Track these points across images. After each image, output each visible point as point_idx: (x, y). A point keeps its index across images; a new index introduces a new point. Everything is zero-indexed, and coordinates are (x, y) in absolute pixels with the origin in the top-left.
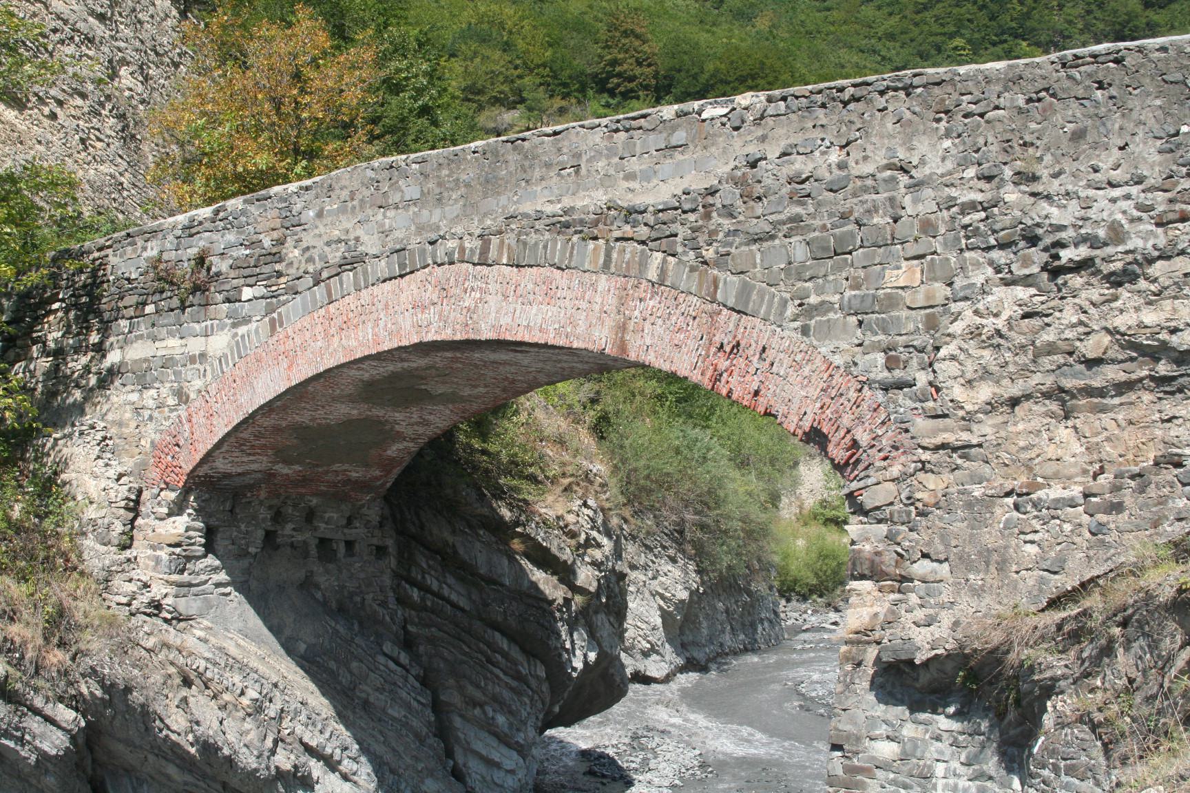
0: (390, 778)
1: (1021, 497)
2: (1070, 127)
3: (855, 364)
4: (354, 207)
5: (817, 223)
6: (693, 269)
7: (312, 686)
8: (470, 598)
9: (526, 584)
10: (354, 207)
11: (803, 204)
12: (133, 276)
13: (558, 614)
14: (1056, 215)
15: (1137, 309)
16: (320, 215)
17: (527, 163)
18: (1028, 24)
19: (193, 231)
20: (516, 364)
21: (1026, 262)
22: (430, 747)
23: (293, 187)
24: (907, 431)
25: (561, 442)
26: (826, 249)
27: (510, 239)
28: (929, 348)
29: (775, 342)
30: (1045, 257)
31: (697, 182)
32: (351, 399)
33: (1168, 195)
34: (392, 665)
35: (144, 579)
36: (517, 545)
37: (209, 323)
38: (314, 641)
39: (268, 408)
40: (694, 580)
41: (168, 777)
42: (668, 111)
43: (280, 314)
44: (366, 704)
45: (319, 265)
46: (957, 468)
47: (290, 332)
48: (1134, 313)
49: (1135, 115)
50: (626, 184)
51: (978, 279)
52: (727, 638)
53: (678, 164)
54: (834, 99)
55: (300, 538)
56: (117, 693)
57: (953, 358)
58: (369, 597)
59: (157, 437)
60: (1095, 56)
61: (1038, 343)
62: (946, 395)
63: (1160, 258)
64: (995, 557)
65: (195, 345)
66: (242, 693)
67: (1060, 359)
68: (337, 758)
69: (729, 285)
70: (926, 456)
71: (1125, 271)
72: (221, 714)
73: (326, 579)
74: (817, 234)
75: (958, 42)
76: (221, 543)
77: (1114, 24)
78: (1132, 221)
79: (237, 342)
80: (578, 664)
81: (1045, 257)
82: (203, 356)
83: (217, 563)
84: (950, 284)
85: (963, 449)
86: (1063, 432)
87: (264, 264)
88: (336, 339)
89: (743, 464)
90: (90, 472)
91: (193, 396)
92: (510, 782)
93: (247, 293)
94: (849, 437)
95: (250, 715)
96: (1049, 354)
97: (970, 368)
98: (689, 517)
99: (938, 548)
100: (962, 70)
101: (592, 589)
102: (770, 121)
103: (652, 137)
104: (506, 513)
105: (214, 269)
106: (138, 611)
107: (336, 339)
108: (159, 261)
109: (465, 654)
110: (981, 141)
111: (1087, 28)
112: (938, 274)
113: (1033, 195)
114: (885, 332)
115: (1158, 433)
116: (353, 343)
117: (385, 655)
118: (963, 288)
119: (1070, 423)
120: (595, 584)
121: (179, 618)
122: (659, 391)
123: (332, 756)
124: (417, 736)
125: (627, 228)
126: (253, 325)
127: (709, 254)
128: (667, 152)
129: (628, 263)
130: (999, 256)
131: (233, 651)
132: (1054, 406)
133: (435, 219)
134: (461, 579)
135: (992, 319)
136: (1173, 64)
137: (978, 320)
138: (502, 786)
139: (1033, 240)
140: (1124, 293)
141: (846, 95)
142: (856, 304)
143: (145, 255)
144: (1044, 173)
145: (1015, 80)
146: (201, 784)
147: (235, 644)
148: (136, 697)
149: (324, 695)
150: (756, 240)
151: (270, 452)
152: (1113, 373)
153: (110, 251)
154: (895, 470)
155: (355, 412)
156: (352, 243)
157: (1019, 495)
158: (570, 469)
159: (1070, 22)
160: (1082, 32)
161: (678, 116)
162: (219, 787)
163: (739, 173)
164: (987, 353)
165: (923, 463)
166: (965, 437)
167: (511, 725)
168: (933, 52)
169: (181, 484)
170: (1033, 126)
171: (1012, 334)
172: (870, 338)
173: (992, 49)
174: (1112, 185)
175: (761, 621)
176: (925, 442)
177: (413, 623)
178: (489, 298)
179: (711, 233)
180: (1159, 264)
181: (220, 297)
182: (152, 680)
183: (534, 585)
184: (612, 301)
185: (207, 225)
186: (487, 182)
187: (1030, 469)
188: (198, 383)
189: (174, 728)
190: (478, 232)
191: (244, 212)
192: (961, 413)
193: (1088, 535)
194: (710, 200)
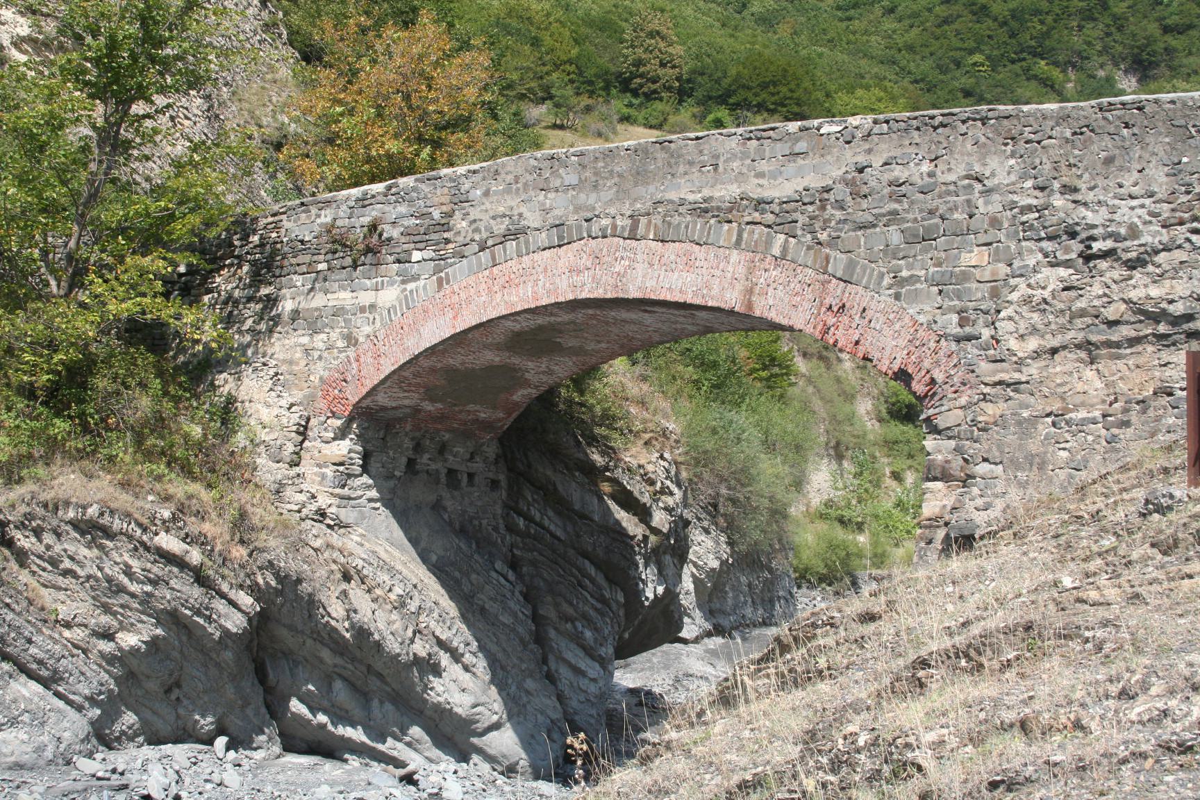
0: (501, 674)
1: (1057, 417)
2: (1103, 155)
3: (935, 322)
4: (518, 189)
5: (910, 216)
6: (809, 248)
7: (443, 591)
8: (565, 530)
9: (612, 521)
10: (518, 189)
11: (900, 202)
12: (307, 239)
13: (637, 549)
14: (1091, 217)
15: (1146, 286)
16: (487, 194)
17: (673, 161)
18: (1047, 43)
19: (366, 202)
20: (640, 323)
21: (1067, 250)
22: (531, 651)
23: (461, 170)
24: (973, 371)
25: (642, 403)
26: (916, 236)
27: (657, 220)
28: (993, 311)
29: (873, 305)
30: (1081, 247)
31: (815, 182)
32: (498, 347)
33: (1172, 206)
34: (502, 581)
35: (313, 491)
36: (606, 487)
37: (380, 279)
38: (443, 553)
39: (431, 351)
40: (725, 551)
41: (321, 661)
42: (793, 126)
43: (447, 274)
44: (483, 610)
45: (484, 235)
46: (1010, 399)
47: (456, 287)
48: (1143, 288)
49: (1150, 148)
50: (756, 181)
51: (1031, 262)
52: (748, 611)
53: (800, 168)
54: (926, 125)
55: (433, 466)
56: (289, 583)
57: (1010, 318)
58: (484, 522)
59: (326, 374)
60: (1123, 104)
61: (1073, 309)
62: (1004, 346)
63: (1163, 250)
64: (1037, 460)
65: (366, 298)
66: (390, 590)
67: (1089, 320)
68: (461, 651)
69: (838, 262)
70: (987, 390)
71: (1138, 259)
72: (374, 606)
74: (909, 224)
75: (978, 58)
76: (374, 465)
77: (1132, 47)
78: (1145, 223)
79: (406, 296)
80: (651, 596)
81: (1081, 247)
82: (373, 307)
83: (371, 482)
84: (1010, 265)
85: (1015, 385)
86: (1089, 374)
87: (433, 233)
89: (769, 446)
90: (264, 401)
91: (361, 339)
93: (416, 256)
94: (928, 376)
95: (396, 608)
96: (1081, 316)
97: (1023, 326)
98: (724, 491)
99: (995, 454)
100: (1025, 108)
101: (665, 530)
102: (875, 138)
103: (779, 145)
104: (597, 458)
105: (385, 235)
106: (307, 517)
107: (499, 295)
108: (333, 226)
109: (560, 576)
110: (1037, 161)
111: (1105, 50)
112: (1002, 257)
113: (1074, 202)
114: (959, 299)
115: (1157, 374)
117: (497, 571)
118: (1019, 268)
119: (1094, 367)
120: (667, 526)
121: (340, 525)
122: (695, 377)
123: (457, 649)
124: (522, 640)
125: (757, 214)
126: (421, 283)
127: (823, 236)
128: (791, 158)
129: (756, 242)
130: (1044, 244)
131: (383, 555)
132: (1083, 355)
133: (591, 201)
134: (559, 514)
135: (1040, 291)
136: (1179, 113)
137: (1030, 291)
138: (585, 692)
139: (1073, 235)
140: (1137, 274)
141: (936, 122)
142: (937, 278)
143: (319, 221)
144: (1083, 187)
145: (1064, 118)
146: (350, 666)
147: (384, 550)
148: (305, 588)
149: (451, 598)
150: (862, 227)
151: (422, 390)
152: (1126, 331)
153: (284, 217)
154: (963, 400)
155: (497, 359)
156: (516, 218)
157: (1056, 416)
158: (651, 426)
159: (1089, 44)
160: (1100, 53)
161: (801, 130)
162: (364, 669)
163: (850, 177)
164: (1035, 316)
165: (984, 395)
166: (1017, 376)
167: (596, 640)
168: (952, 66)
169: (347, 413)
170: (1076, 152)
171: (1055, 302)
172: (947, 303)
173: (1010, 67)
174: (1131, 197)
175: (779, 598)
176: (987, 380)
177: (518, 548)
178: (636, 265)
179: (825, 221)
180: (1163, 254)
181: (391, 259)
182: (318, 574)
183: (618, 523)
184: (741, 271)
185: (380, 198)
186: (638, 173)
187: (1063, 399)
188: (367, 329)
189: (334, 615)
190: (629, 213)
191: (414, 189)
192: (1015, 359)
193: (1104, 443)
194: (826, 196)
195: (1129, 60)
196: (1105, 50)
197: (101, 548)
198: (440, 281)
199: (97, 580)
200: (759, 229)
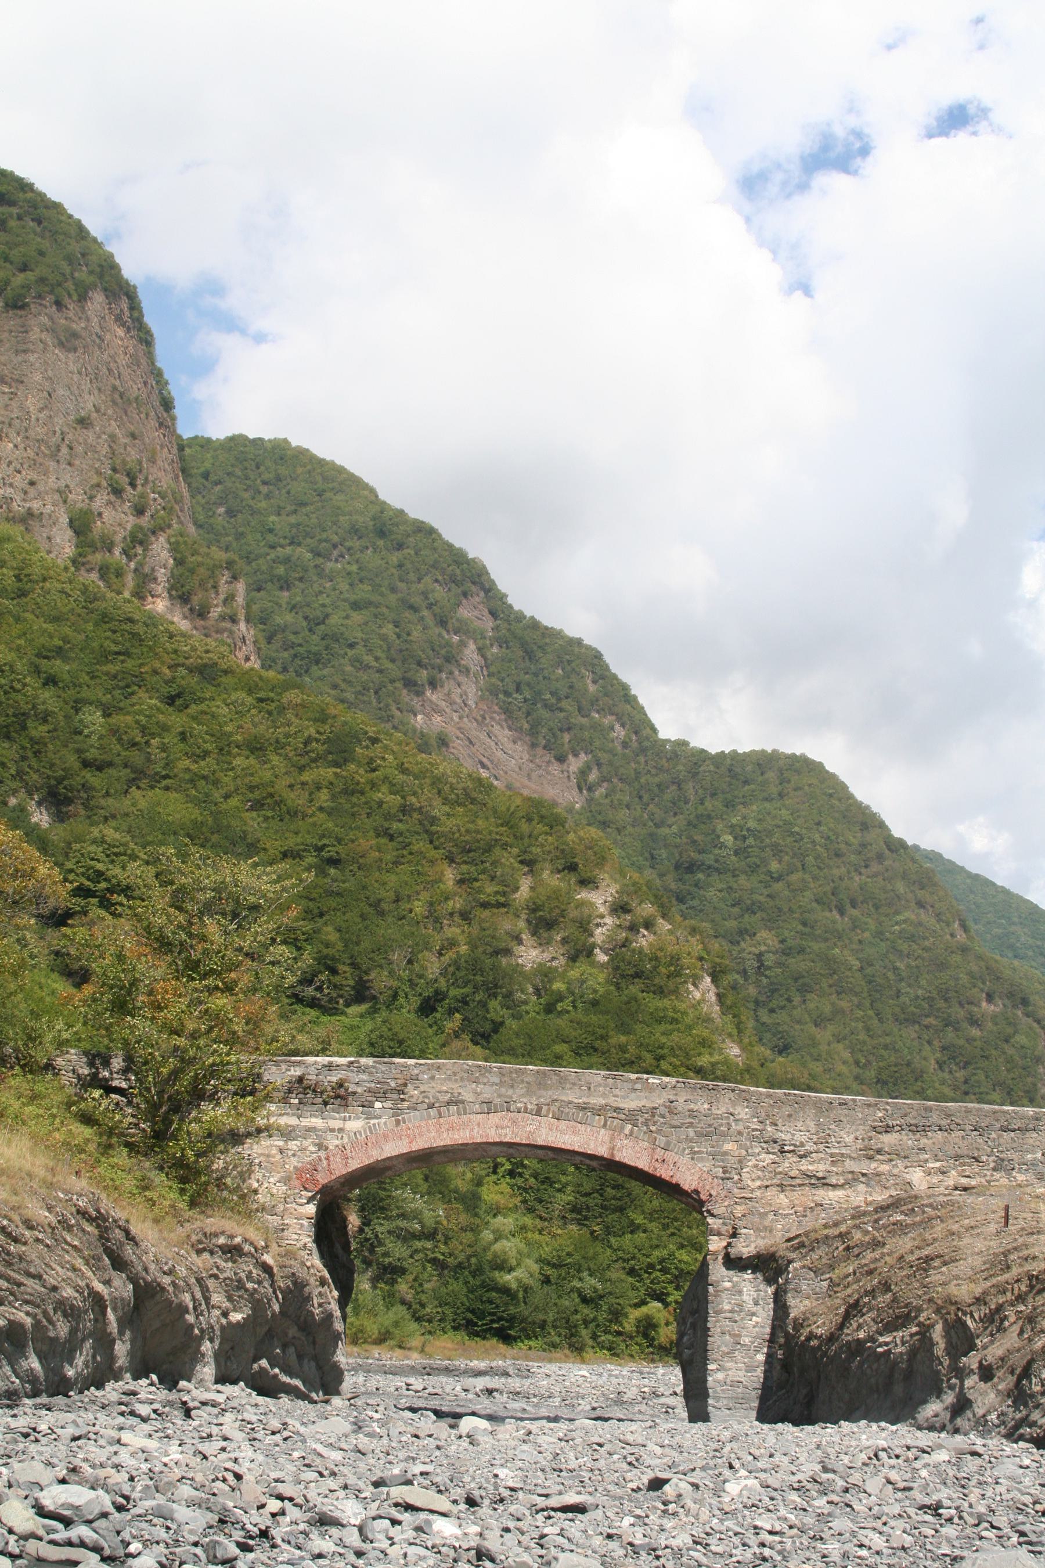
16: (433, 1078)
23: (411, 1062)
31: (649, 1105)
41: (286, 1335)
42: (633, 1076)
48: (805, 1166)
69: (661, 1140)
77: (48, 777)
82: (341, 1130)
86: (782, 1196)
88: (445, 1135)
107: (445, 1135)
111: (20, 775)
116: (456, 1137)
127: (653, 1128)
139: (775, 1142)
145: (769, 1096)
152: (798, 1181)
184: (607, 1139)
188: (337, 1142)
195: (45, 791)
196: (20, 775)
197: (234, 1262)
198: (398, 1122)
199: (231, 1280)
200: (616, 1121)
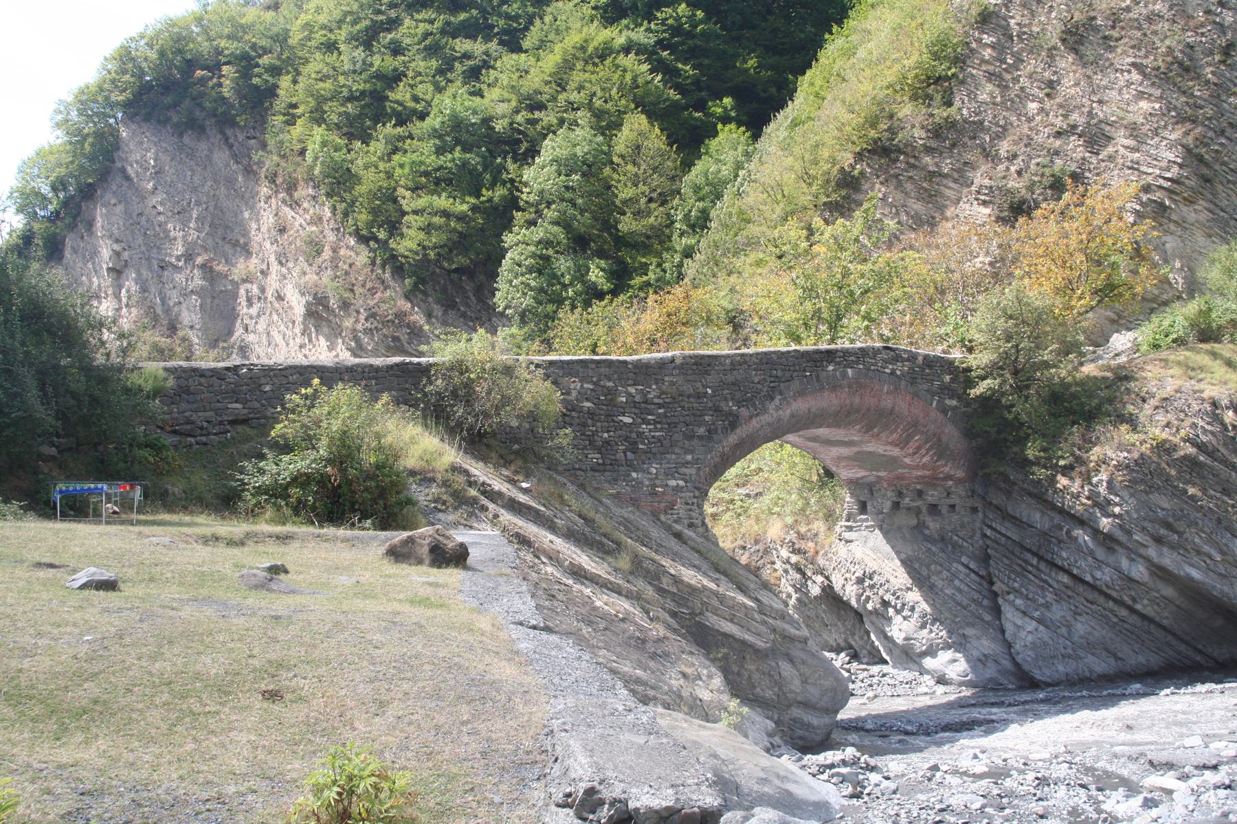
44: (932, 587)
73: (933, 525)
92: (1030, 638)
